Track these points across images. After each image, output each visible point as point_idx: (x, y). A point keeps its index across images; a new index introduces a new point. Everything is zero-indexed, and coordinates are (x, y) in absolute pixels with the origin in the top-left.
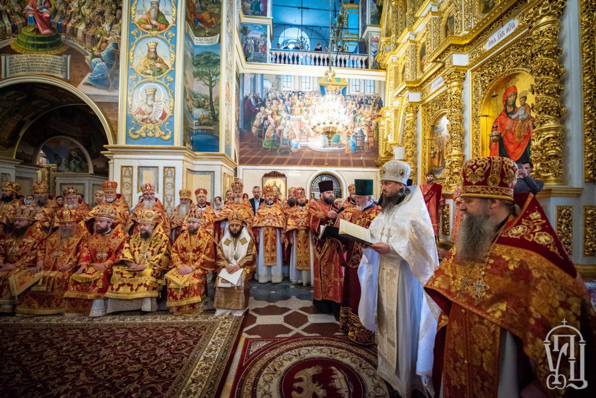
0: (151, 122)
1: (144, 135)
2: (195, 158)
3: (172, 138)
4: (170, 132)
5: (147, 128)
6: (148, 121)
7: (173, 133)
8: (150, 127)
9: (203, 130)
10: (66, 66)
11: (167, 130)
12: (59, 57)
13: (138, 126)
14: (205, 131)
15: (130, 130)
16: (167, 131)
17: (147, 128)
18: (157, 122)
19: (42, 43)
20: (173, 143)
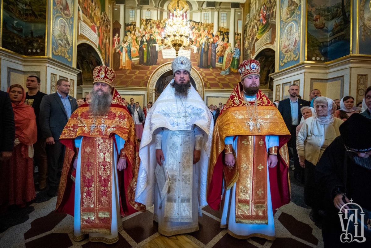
0: (289, 51)
1: (286, 62)
2: (326, 68)
3: (299, 58)
4: (298, 53)
5: (287, 56)
6: (288, 51)
7: (299, 53)
8: (288, 54)
9: (336, 38)
10: (270, 35)
11: (297, 52)
12: (268, 32)
13: (284, 57)
14: (337, 39)
15: (281, 61)
16: (297, 53)
17: (287, 56)
18: (292, 49)
19: (264, 29)
20: (299, 62)
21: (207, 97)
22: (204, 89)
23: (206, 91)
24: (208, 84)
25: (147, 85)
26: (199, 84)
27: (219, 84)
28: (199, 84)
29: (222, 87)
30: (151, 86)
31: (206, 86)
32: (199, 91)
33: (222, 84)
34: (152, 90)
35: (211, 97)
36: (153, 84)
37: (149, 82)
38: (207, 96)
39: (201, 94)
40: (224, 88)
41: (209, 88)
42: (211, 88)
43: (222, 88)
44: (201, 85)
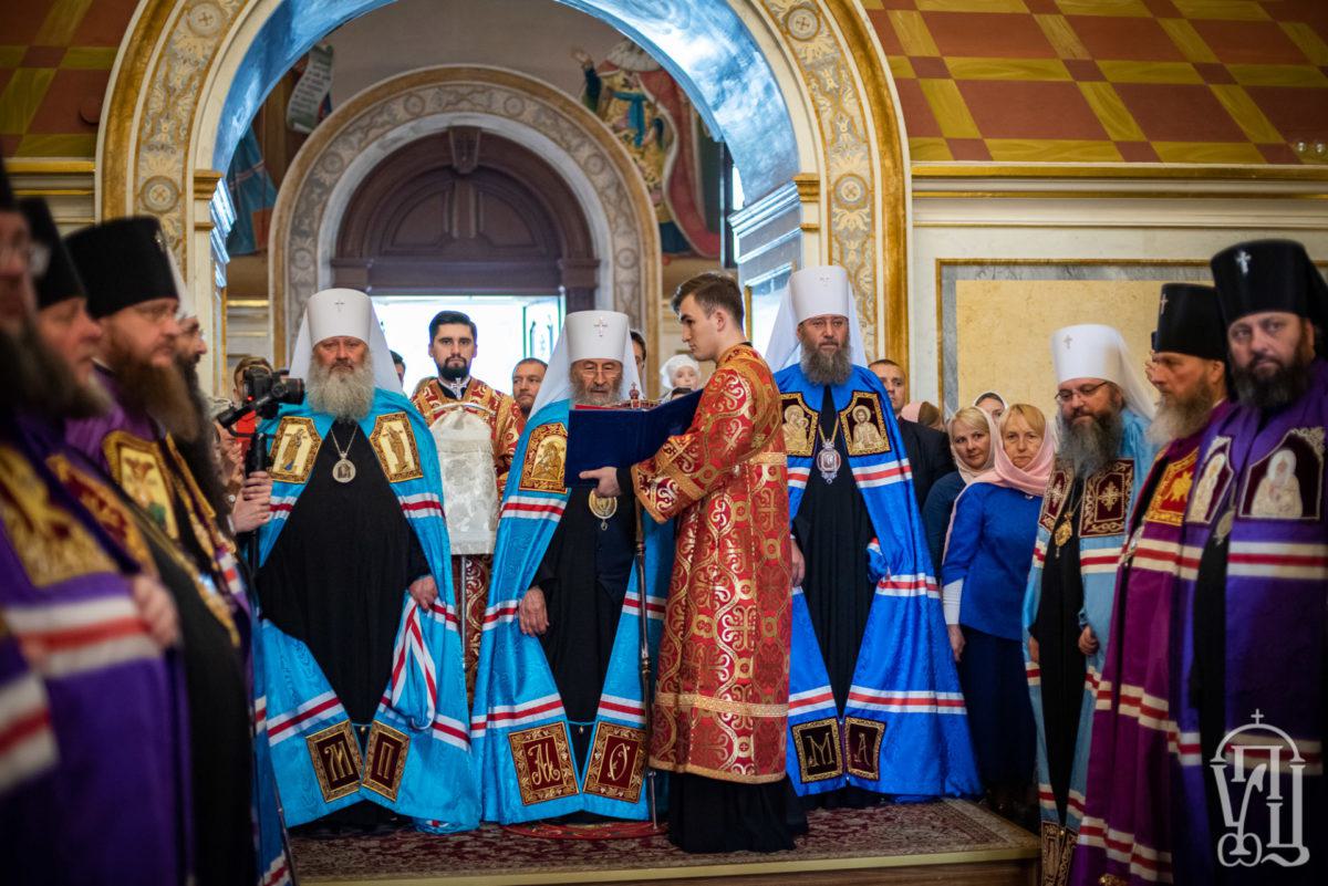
21: (942, 264)
22: (909, 168)
23: (935, 189)
24: (946, 99)
25: (93, 126)
26: (835, 96)
27: (1086, 88)
28: (835, 96)
29: (1134, 133)
30: (161, 138)
31: (922, 123)
32: (834, 197)
33: (1131, 94)
34: (179, 195)
35: (995, 263)
36: (185, 103)
37: (130, 80)
38: (948, 255)
39: (870, 235)
40: (1159, 147)
41: (961, 149)
42: (989, 142)
43: (1129, 150)
44: (858, 105)
